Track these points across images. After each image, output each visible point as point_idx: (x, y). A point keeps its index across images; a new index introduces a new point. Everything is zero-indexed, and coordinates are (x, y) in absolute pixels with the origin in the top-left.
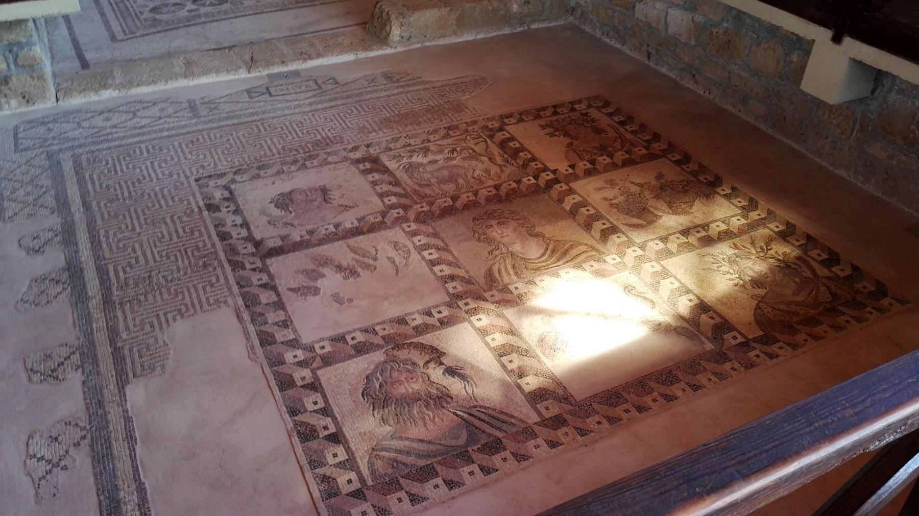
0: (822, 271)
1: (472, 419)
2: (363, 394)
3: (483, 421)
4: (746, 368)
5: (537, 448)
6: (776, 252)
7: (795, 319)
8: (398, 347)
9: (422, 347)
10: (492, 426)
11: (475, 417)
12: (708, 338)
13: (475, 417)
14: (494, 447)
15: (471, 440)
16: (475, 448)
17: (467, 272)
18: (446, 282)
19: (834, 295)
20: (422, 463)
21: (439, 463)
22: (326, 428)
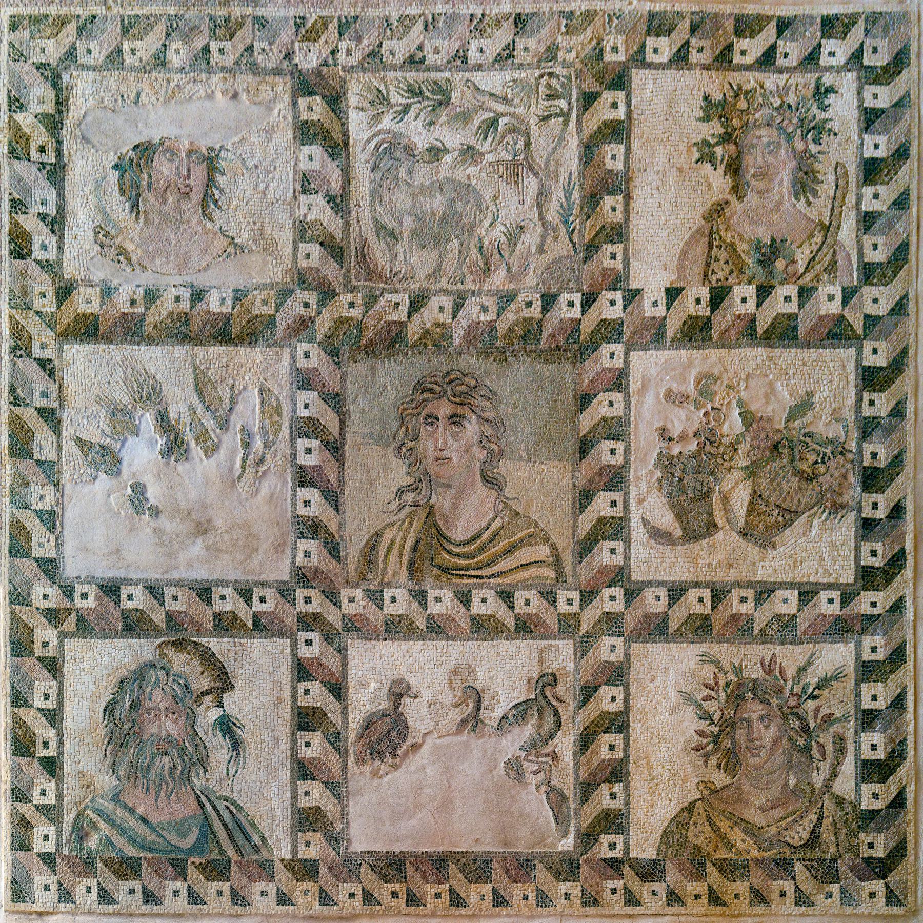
0: (845, 784)
1: (213, 814)
2: (105, 710)
3: (225, 825)
4: (585, 904)
5: (262, 895)
6: (817, 710)
7: (722, 854)
8: (179, 645)
9: (208, 659)
10: (231, 838)
11: (219, 815)
12: (578, 831)
13: (219, 815)
14: (217, 870)
15: (197, 848)
16: (197, 861)
17: (341, 525)
18: (302, 536)
19: (814, 838)
20: (131, 851)
21: (149, 861)
22: (46, 745)
